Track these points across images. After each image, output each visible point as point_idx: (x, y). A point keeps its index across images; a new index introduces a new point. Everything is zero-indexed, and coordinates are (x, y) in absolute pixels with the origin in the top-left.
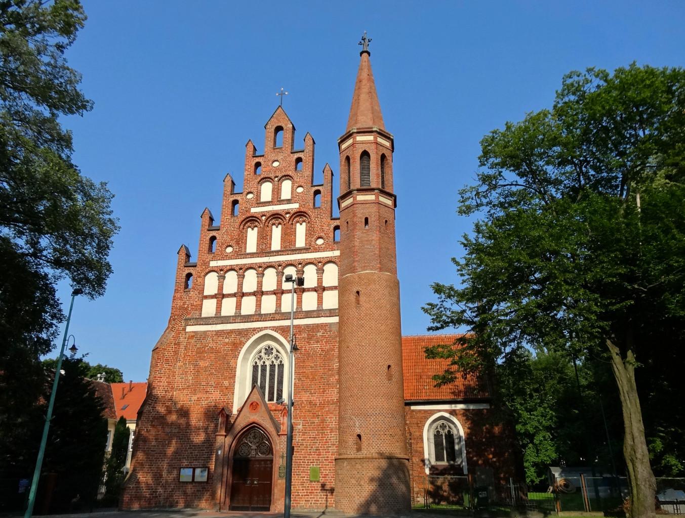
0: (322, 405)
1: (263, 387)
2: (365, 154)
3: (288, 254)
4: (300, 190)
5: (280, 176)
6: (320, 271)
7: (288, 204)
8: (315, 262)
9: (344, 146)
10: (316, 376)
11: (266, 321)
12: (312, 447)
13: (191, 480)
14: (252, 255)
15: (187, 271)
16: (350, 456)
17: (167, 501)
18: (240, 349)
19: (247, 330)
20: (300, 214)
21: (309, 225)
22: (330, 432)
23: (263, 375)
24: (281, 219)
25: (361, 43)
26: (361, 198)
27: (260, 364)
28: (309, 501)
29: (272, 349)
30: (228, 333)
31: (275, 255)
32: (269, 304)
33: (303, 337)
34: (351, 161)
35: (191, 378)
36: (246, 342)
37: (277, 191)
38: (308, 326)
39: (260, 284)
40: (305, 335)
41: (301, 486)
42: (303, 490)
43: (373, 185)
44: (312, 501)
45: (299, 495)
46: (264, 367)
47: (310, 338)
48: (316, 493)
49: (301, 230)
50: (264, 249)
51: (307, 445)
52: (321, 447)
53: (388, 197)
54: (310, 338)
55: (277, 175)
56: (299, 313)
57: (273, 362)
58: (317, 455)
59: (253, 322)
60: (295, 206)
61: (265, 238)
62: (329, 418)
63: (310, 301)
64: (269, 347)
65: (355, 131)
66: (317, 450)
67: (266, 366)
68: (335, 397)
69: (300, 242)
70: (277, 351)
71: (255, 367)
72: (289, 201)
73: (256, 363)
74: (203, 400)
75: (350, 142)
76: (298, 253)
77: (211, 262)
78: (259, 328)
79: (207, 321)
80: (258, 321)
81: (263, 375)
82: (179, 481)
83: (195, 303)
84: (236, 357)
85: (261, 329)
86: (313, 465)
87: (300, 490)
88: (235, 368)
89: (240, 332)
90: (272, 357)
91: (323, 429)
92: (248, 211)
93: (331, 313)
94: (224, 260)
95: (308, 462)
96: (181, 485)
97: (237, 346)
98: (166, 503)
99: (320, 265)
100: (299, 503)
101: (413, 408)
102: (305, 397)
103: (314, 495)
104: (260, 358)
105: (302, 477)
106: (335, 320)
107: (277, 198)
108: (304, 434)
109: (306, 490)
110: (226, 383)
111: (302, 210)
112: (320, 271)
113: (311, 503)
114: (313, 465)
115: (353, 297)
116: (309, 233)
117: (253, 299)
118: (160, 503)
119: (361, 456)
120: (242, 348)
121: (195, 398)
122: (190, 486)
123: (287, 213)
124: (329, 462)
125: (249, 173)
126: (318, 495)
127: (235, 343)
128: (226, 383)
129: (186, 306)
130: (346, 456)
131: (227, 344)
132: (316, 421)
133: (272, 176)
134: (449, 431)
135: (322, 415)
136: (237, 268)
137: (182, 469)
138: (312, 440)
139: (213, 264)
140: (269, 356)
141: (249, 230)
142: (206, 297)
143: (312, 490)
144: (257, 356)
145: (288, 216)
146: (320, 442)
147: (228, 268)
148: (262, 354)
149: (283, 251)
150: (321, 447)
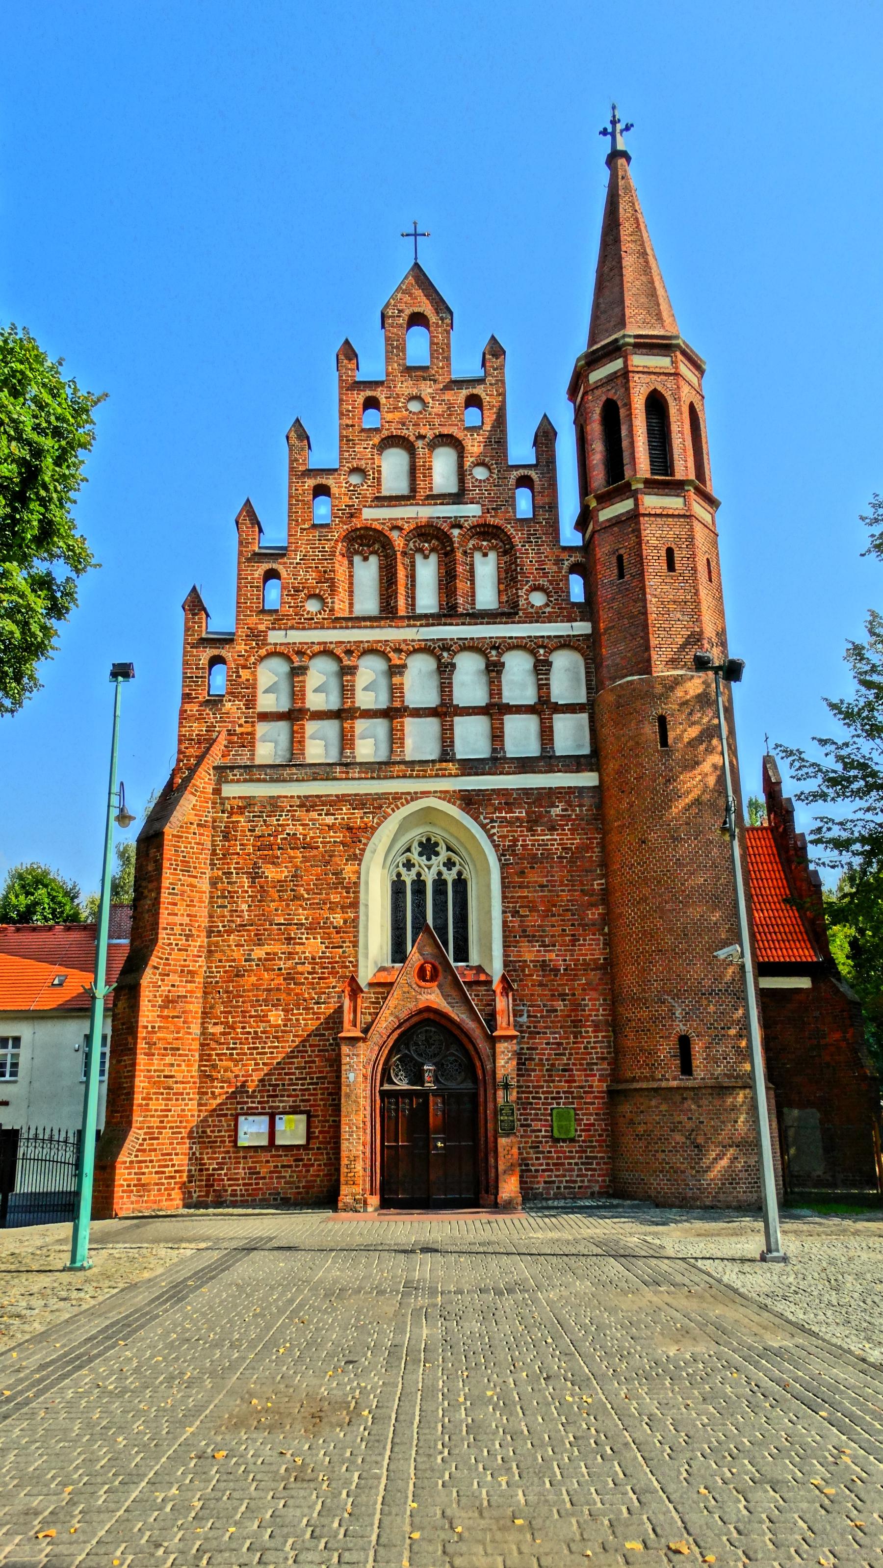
0: (571, 973)
1: (442, 930)
2: (657, 405)
3: (463, 624)
5: (430, 435)
6: (542, 668)
7: (454, 504)
9: (596, 376)
10: (555, 906)
11: (424, 777)
12: (553, 1065)
13: (265, 1142)
15: (210, 652)
16: (664, 1084)
17: (208, 1193)
18: (364, 841)
20: (488, 533)
21: (506, 558)
22: (594, 1032)
23: (419, 906)
24: (438, 539)
25: (604, 132)
26: (651, 502)
27: (408, 878)
28: (554, 1182)
29: (437, 844)
30: (332, 803)
31: (433, 625)
33: (518, 818)
34: (622, 412)
35: (245, 907)
36: (379, 825)
38: (527, 792)
40: (520, 813)
41: (531, 1151)
42: (538, 1159)
43: (679, 475)
44: (561, 1182)
45: (530, 1171)
46: (419, 886)
47: (532, 822)
48: (570, 1164)
51: (541, 1060)
52: (574, 1064)
53: (706, 506)
55: (423, 432)
57: (440, 874)
58: (566, 1081)
59: (392, 777)
60: (471, 511)
62: (589, 1000)
63: (521, 737)
64: (429, 840)
65: (632, 340)
66: (564, 1070)
67: (424, 882)
68: (602, 954)
72: (458, 498)
73: (399, 875)
74: (280, 959)
75: (617, 365)
76: (488, 623)
77: (271, 633)
78: (409, 793)
79: (274, 772)
80: (404, 777)
81: (419, 906)
82: (236, 1146)
83: (239, 730)
84: (357, 859)
85: (414, 797)
86: (558, 1104)
87: (532, 1159)
88: (357, 884)
89: (359, 802)
90: (438, 862)
91: (576, 1023)
94: (304, 629)
95: (546, 1098)
96: (241, 1154)
97: (356, 838)
98: (207, 1196)
99: (540, 654)
100: (532, 1189)
102: (529, 953)
103: (565, 1170)
104: (409, 865)
105: (534, 1131)
106: (588, 779)
108: (533, 1035)
109: (544, 1158)
110: (337, 919)
113: (559, 1188)
114: (558, 1104)
115: (650, 731)
116: (509, 578)
117: (331, 728)
118: (191, 1197)
119: (690, 1084)
120: (369, 839)
121: (259, 953)
122: (264, 1156)
123: (454, 526)
124: (596, 1097)
125: (350, 422)
126: (573, 1170)
127: (350, 829)
128: (337, 919)
129: (215, 735)
130: (644, 1085)
131: (330, 827)
132: (560, 1005)
133: (410, 433)
135: (574, 995)
136: (338, 651)
137: (241, 1119)
138: (551, 1049)
139: (275, 637)
140: (429, 859)
142: (265, 717)
143: (559, 1158)
144: (402, 859)
145: (456, 532)
146: (570, 1054)
147: (316, 648)
148: (415, 856)
149: (450, 616)
150: (574, 1064)
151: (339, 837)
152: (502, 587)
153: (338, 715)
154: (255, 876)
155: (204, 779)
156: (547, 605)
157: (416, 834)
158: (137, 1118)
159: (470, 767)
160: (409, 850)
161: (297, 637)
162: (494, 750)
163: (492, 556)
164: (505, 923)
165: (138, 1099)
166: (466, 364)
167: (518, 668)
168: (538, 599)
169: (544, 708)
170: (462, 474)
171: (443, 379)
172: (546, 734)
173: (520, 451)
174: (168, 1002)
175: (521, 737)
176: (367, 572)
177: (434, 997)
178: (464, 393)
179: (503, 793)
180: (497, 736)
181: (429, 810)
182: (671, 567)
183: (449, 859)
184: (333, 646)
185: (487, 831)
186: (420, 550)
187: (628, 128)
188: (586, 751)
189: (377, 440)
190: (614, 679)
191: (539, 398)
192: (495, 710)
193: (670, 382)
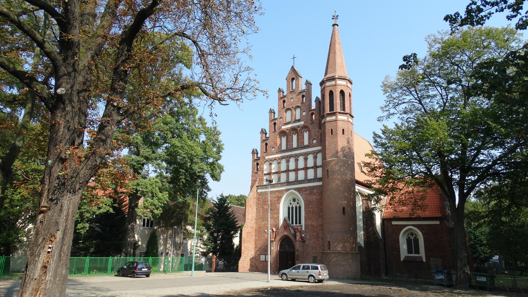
2: (331, 93)
4: (304, 114)
6: (315, 157)
19: (283, 190)
20: (305, 127)
26: (328, 119)
27: (291, 206)
32: (292, 176)
38: (309, 187)
39: (288, 166)
40: (308, 192)
46: (292, 208)
47: (311, 193)
49: (306, 135)
54: (311, 193)
60: (302, 123)
61: (289, 142)
63: (311, 174)
69: (306, 142)
71: (289, 208)
72: (299, 121)
90: (296, 203)
93: (320, 180)
97: (279, 198)
99: (315, 154)
101: (394, 223)
104: (291, 204)
108: (310, 240)
110: (276, 216)
111: (306, 125)
112: (315, 157)
121: (263, 223)
128: (276, 216)
132: (315, 234)
134: (416, 237)
139: (267, 158)
151: (275, 199)
154: (263, 208)
155: (255, 188)
157: (291, 197)
158: (242, 255)
161: (270, 157)
165: (242, 251)
166: (303, 87)
169: (315, 167)
171: (297, 93)
172: (316, 173)
173: (314, 106)
174: (248, 233)
176: (284, 140)
177: (286, 233)
178: (301, 95)
179: (305, 188)
180: (306, 174)
181: (292, 193)
182: (332, 134)
187: (337, 16)
189: (285, 110)
191: (316, 93)
193: (334, 87)
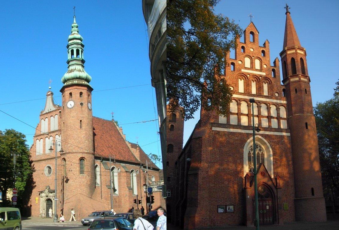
6: (278, 109)
7: (260, 72)
8: (276, 104)
14: (241, 94)
20: (266, 79)
21: (270, 85)
31: (256, 97)
37: (252, 63)
49: (265, 86)
50: (247, 92)
56: (269, 129)
60: (264, 74)
63: (274, 123)
69: (266, 93)
70: (260, 147)
92: (240, 70)
99: (277, 106)
107: (252, 67)
111: (267, 77)
115: (305, 125)
141: (239, 80)
144: (250, 149)
152: (269, 91)
153: (237, 114)
156: (279, 96)
159: (265, 129)
160: (251, 146)
162: (269, 126)
163: (267, 84)
164: (273, 164)
167: (273, 108)
168: (277, 95)
170: (261, 66)
175: (274, 123)
183: (260, 149)
184: (236, 98)
185: (269, 144)
186: (253, 80)
188: (287, 128)
190: (295, 114)
192: (269, 117)
